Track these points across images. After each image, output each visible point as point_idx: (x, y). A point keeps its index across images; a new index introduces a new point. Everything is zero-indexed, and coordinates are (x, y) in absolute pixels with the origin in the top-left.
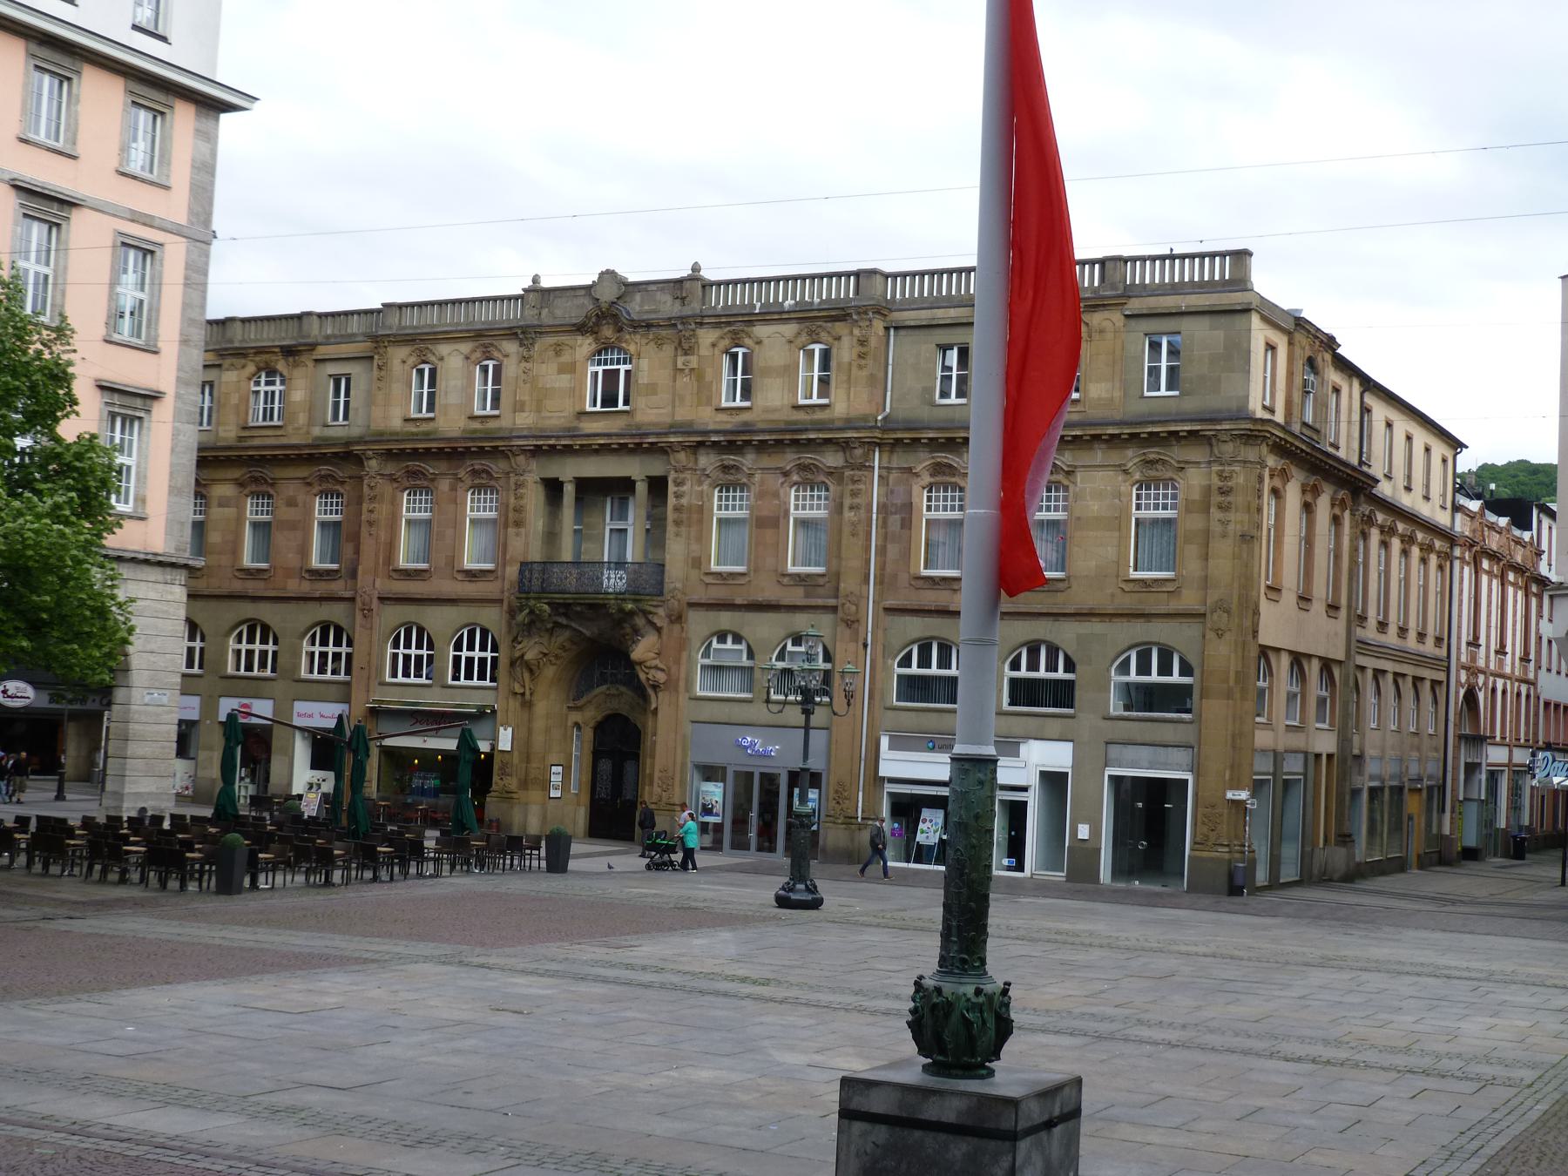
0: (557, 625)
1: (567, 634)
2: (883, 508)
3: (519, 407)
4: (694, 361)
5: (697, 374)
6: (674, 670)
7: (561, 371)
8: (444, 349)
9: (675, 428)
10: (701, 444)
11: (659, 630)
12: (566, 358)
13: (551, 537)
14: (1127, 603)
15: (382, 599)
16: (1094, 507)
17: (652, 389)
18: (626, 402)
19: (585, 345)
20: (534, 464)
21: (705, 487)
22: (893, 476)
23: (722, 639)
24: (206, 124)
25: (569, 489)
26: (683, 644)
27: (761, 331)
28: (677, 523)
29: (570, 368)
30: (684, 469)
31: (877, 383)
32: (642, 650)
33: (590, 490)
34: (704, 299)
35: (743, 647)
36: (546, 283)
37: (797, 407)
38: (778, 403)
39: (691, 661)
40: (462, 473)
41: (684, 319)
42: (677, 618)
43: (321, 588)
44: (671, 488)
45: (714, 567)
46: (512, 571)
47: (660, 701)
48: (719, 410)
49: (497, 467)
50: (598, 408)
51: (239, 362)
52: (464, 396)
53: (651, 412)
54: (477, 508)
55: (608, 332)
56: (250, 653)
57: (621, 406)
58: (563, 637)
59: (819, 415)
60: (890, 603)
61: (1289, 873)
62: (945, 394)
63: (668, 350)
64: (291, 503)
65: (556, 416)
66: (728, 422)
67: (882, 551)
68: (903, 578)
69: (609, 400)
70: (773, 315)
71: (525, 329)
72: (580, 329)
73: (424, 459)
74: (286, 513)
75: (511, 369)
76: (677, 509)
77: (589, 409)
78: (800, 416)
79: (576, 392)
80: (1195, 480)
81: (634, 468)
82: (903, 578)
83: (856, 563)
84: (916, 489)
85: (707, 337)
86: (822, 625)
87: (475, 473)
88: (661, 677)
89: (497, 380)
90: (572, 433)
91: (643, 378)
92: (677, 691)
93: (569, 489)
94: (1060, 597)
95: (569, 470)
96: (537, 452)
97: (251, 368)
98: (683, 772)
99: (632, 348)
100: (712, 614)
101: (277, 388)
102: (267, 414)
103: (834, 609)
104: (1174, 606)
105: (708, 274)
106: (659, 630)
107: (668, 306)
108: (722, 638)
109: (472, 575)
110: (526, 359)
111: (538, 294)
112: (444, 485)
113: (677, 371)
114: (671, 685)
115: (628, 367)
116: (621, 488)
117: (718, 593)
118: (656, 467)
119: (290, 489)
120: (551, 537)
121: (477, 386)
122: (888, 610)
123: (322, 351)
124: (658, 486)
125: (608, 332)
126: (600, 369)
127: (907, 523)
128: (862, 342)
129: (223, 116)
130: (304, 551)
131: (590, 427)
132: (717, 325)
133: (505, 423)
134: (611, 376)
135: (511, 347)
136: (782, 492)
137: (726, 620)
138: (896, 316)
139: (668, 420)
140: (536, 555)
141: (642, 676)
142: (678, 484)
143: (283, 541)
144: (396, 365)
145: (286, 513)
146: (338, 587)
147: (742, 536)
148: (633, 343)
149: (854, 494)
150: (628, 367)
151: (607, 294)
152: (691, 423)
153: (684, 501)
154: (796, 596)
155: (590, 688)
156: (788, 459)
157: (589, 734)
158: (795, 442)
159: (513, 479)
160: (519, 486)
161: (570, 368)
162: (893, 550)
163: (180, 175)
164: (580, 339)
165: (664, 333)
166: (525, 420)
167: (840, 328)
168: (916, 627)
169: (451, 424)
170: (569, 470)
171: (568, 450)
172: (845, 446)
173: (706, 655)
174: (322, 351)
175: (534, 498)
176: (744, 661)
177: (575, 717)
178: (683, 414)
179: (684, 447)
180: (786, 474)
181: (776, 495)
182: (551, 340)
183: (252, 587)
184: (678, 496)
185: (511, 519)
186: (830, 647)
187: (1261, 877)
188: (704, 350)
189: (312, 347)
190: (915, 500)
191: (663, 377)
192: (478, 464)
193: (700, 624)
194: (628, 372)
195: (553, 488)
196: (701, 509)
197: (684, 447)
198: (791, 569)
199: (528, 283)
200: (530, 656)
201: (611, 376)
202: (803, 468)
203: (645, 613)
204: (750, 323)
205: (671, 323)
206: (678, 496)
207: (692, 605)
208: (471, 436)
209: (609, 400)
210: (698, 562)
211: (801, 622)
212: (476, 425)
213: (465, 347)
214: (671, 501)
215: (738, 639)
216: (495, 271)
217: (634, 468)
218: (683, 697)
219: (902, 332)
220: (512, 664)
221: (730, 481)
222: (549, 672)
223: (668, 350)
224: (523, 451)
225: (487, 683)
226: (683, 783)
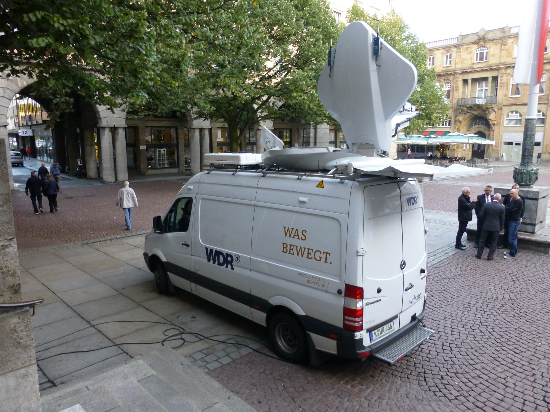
0: (467, 112)
1: (469, 114)
4: (506, 47)
6: (499, 121)
7: (468, 54)
8: (436, 52)
9: (499, 64)
11: (495, 112)
12: (470, 50)
13: (463, 93)
17: (494, 55)
18: (486, 59)
19: (475, 47)
20: (461, 76)
23: (512, 112)
25: (470, 81)
26: (501, 115)
28: (501, 86)
29: (471, 53)
30: (503, 73)
32: (492, 116)
33: (475, 80)
34: (510, 31)
35: (518, 114)
36: (463, 34)
39: (503, 118)
40: (441, 80)
41: (504, 37)
42: (501, 109)
44: (499, 78)
47: (495, 128)
49: (451, 77)
50: (478, 61)
53: (493, 61)
55: (482, 43)
57: (484, 60)
58: (468, 115)
61: (346, 322)
63: (499, 45)
65: (467, 65)
69: (481, 59)
71: (459, 45)
72: (474, 43)
75: (454, 55)
76: (501, 83)
77: (475, 62)
79: (471, 59)
81: (489, 75)
85: (510, 41)
87: (445, 80)
88: (496, 122)
89: (450, 58)
92: (500, 125)
93: (470, 81)
95: (470, 77)
98: (501, 143)
99: (488, 46)
100: (510, 107)
103: (547, 103)
106: (495, 112)
107: (499, 35)
108: (512, 112)
110: (459, 52)
113: (501, 50)
114: (499, 124)
115: (487, 51)
118: (495, 74)
121: (445, 60)
124: (495, 79)
125: (482, 43)
131: (476, 66)
133: (453, 67)
134: (482, 54)
135: (455, 50)
137: (514, 108)
139: (498, 62)
140: (460, 97)
141: (491, 122)
142: (501, 77)
148: (488, 45)
150: (487, 51)
151: (481, 34)
152: (505, 62)
155: (472, 126)
159: (455, 80)
160: (456, 81)
164: (473, 46)
165: (497, 41)
166: (458, 66)
170: (470, 77)
171: (471, 72)
173: (508, 116)
175: (461, 83)
176: (519, 118)
178: (503, 60)
179: (504, 68)
182: (465, 47)
186: (545, 113)
187: (347, 317)
191: (497, 52)
192: (446, 77)
193: (506, 110)
194: (487, 52)
195: (465, 81)
196: (507, 83)
197: (504, 68)
200: (460, 120)
201: (482, 54)
203: (492, 108)
205: (500, 39)
206: (501, 80)
207: (504, 105)
208: (444, 71)
209: (481, 59)
210: (506, 95)
212: (445, 69)
213: (442, 51)
214: (499, 81)
215: (517, 112)
217: (489, 75)
218: (501, 127)
220: (455, 121)
222: (464, 123)
223: (499, 45)
225: (448, 126)
226: (501, 146)
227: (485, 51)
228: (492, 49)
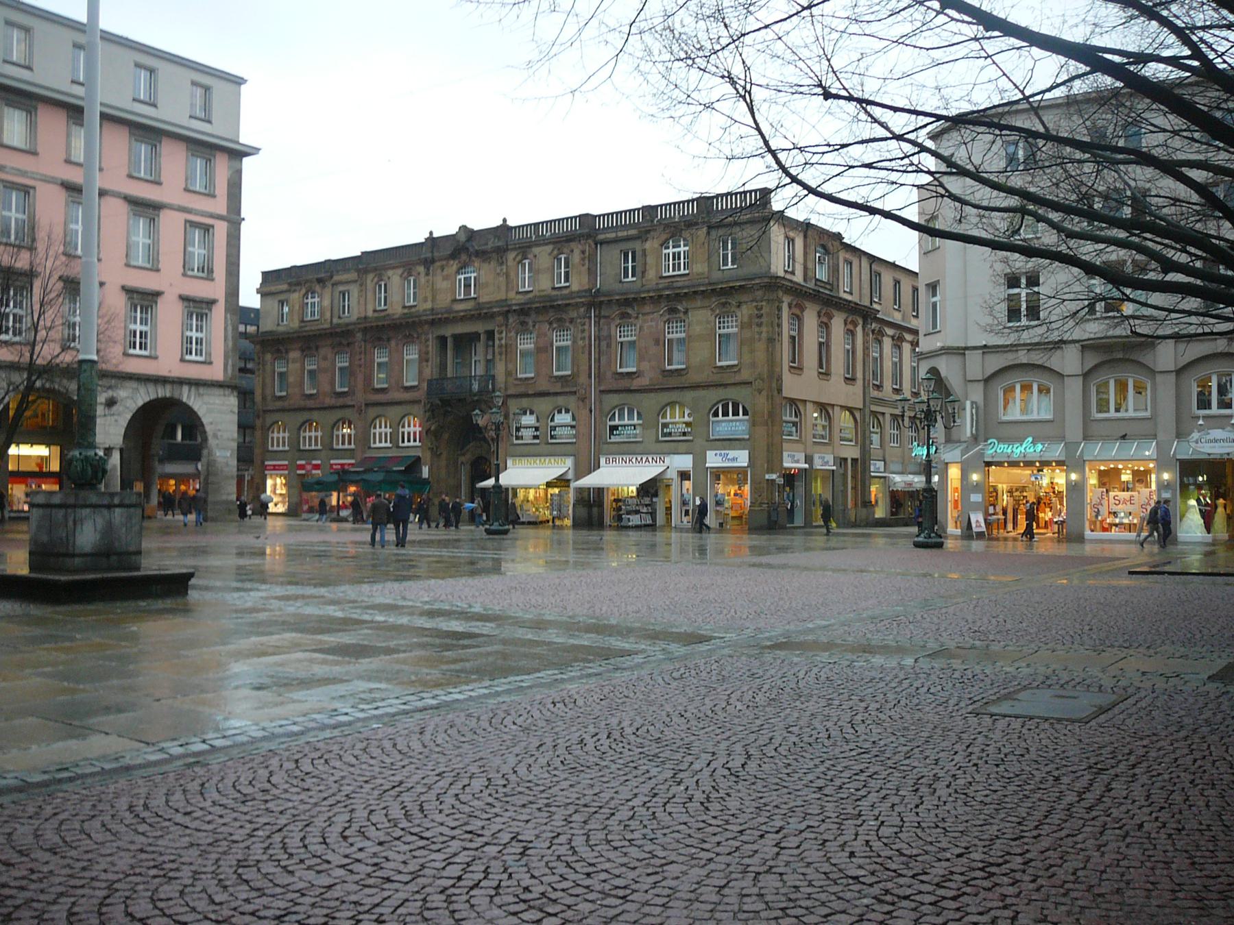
2: (598, 338)
3: (425, 300)
5: (507, 275)
8: (390, 273)
10: (508, 311)
12: (445, 273)
13: (443, 366)
14: (716, 378)
15: (367, 405)
16: (697, 329)
17: (487, 285)
19: (454, 265)
21: (513, 334)
22: (602, 321)
24: (235, 164)
25: (450, 341)
27: (536, 250)
31: (592, 273)
37: (554, 288)
38: (543, 287)
43: (341, 401)
44: (497, 336)
45: (519, 376)
46: (425, 385)
48: (518, 293)
51: (298, 288)
52: (401, 295)
54: (411, 354)
56: (310, 438)
59: (565, 292)
60: (602, 388)
62: (626, 276)
64: (325, 358)
65: (443, 301)
66: (521, 299)
67: (598, 361)
68: (609, 374)
70: (542, 242)
73: (385, 330)
74: (324, 364)
76: (500, 346)
78: (555, 293)
80: (746, 311)
81: (480, 327)
82: (609, 374)
83: (585, 368)
84: (613, 327)
86: (572, 401)
90: (449, 311)
91: (483, 280)
93: (450, 341)
94: (683, 379)
96: (433, 323)
97: (304, 291)
100: (519, 400)
101: (316, 300)
102: (313, 314)
103: (575, 393)
104: (738, 378)
105: (511, 223)
109: (408, 389)
111: (432, 241)
112: (393, 343)
116: (474, 337)
117: (522, 390)
119: (323, 351)
120: (443, 366)
122: (601, 392)
123: (336, 278)
124: (490, 335)
126: (462, 277)
127: (609, 346)
128: (583, 252)
129: (245, 160)
130: (332, 383)
132: (515, 249)
136: (549, 333)
137: (525, 402)
138: (601, 237)
143: (323, 379)
144: (369, 282)
145: (324, 364)
146: (348, 401)
147: (531, 360)
149: (583, 331)
153: (503, 342)
154: (558, 388)
156: (551, 315)
157: (468, 467)
158: (552, 307)
161: (446, 278)
162: (604, 359)
163: (221, 188)
167: (573, 245)
168: (615, 399)
169: (396, 310)
172: (577, 306)
174: (336, 278)
175: (432, 347)
177: (462, 459)
179: (500, 314)
180: (551, 324)
181: (546, 335)
183: (310, 403)
184: (500, 339)
185: (424, 359)
188: (510, 263)
189: (331, 277)
190: (613, 333)
193: (514, 406)
195: (443, 340)
198: (556, 373)
199: (427, 235)
202: (559, 320)
204: (530, 247)
211: (560, 400)
212: (406, 311)
214: (497, 342)
216: (409, 233)
217: (480, 327)
219: (604, 246)
221: (523, 328)
224: (426, 322)
227: (473, 275)
228: (482, 272)
